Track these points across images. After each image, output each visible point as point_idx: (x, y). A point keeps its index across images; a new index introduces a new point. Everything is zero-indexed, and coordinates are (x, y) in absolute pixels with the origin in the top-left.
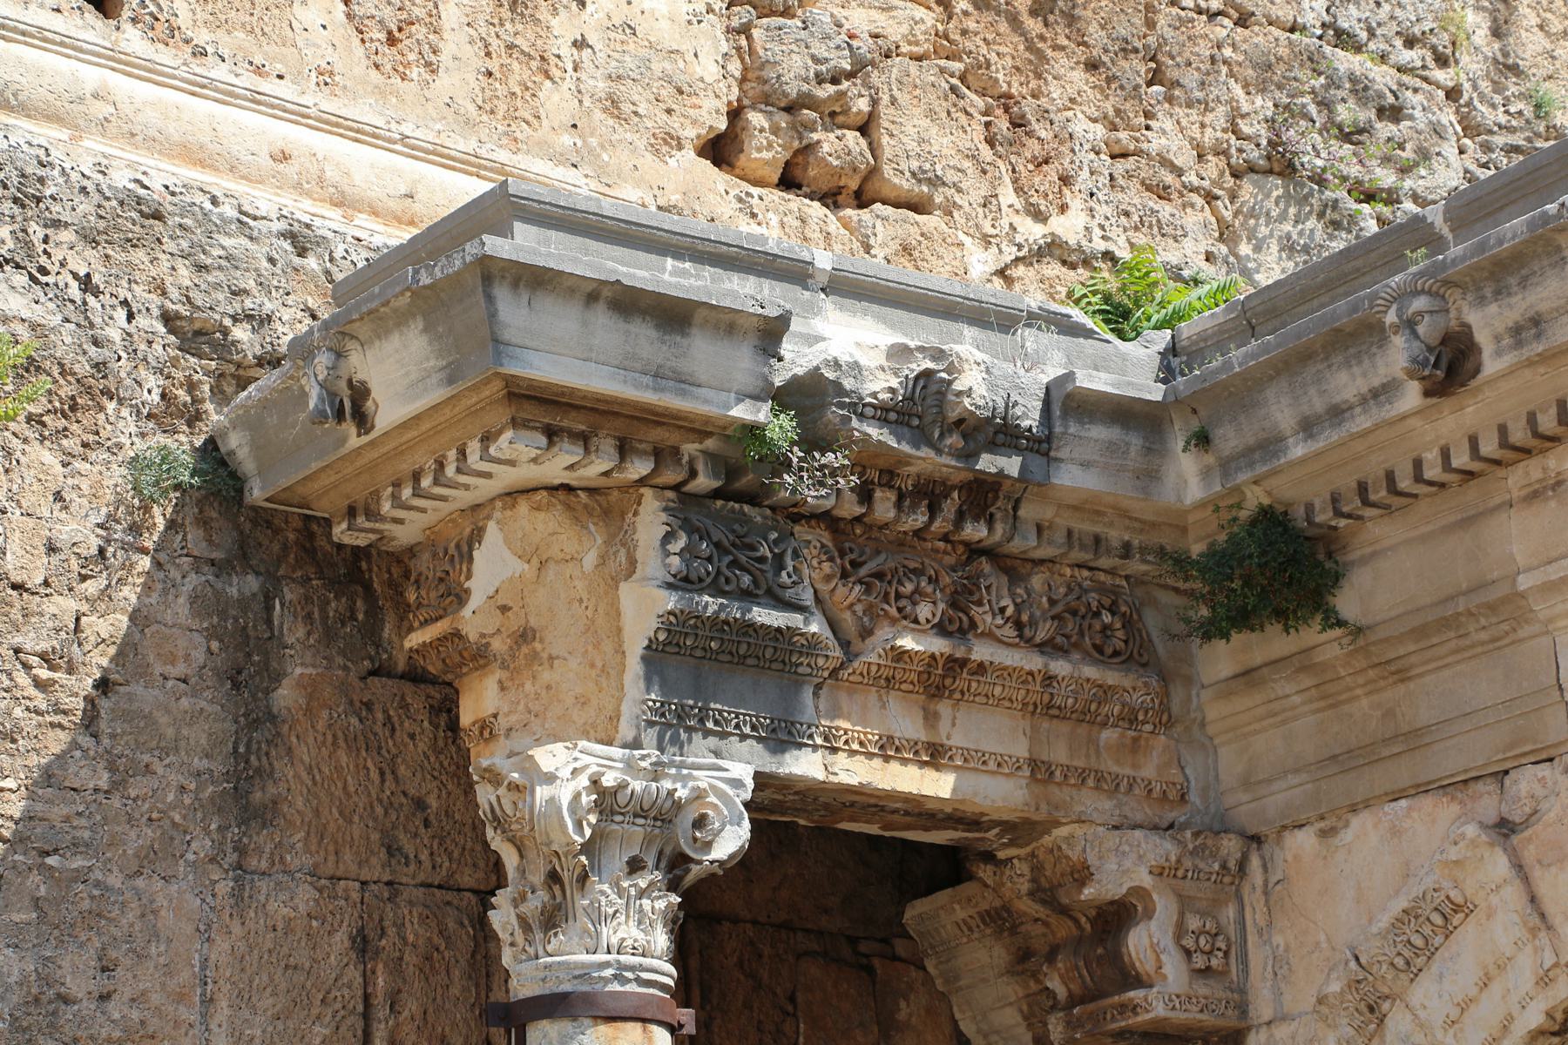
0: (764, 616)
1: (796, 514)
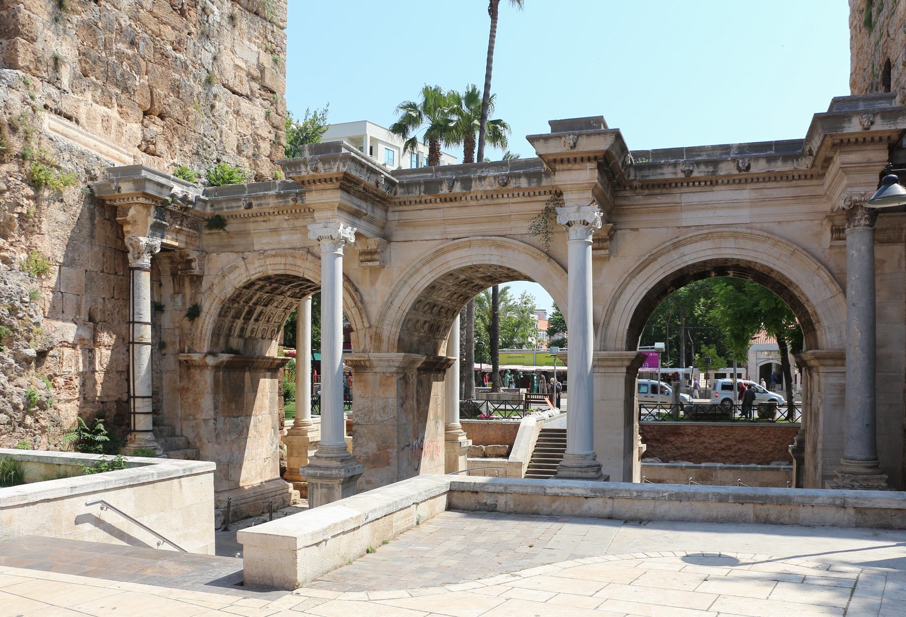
0: (164, 223)
1: (167, 210)
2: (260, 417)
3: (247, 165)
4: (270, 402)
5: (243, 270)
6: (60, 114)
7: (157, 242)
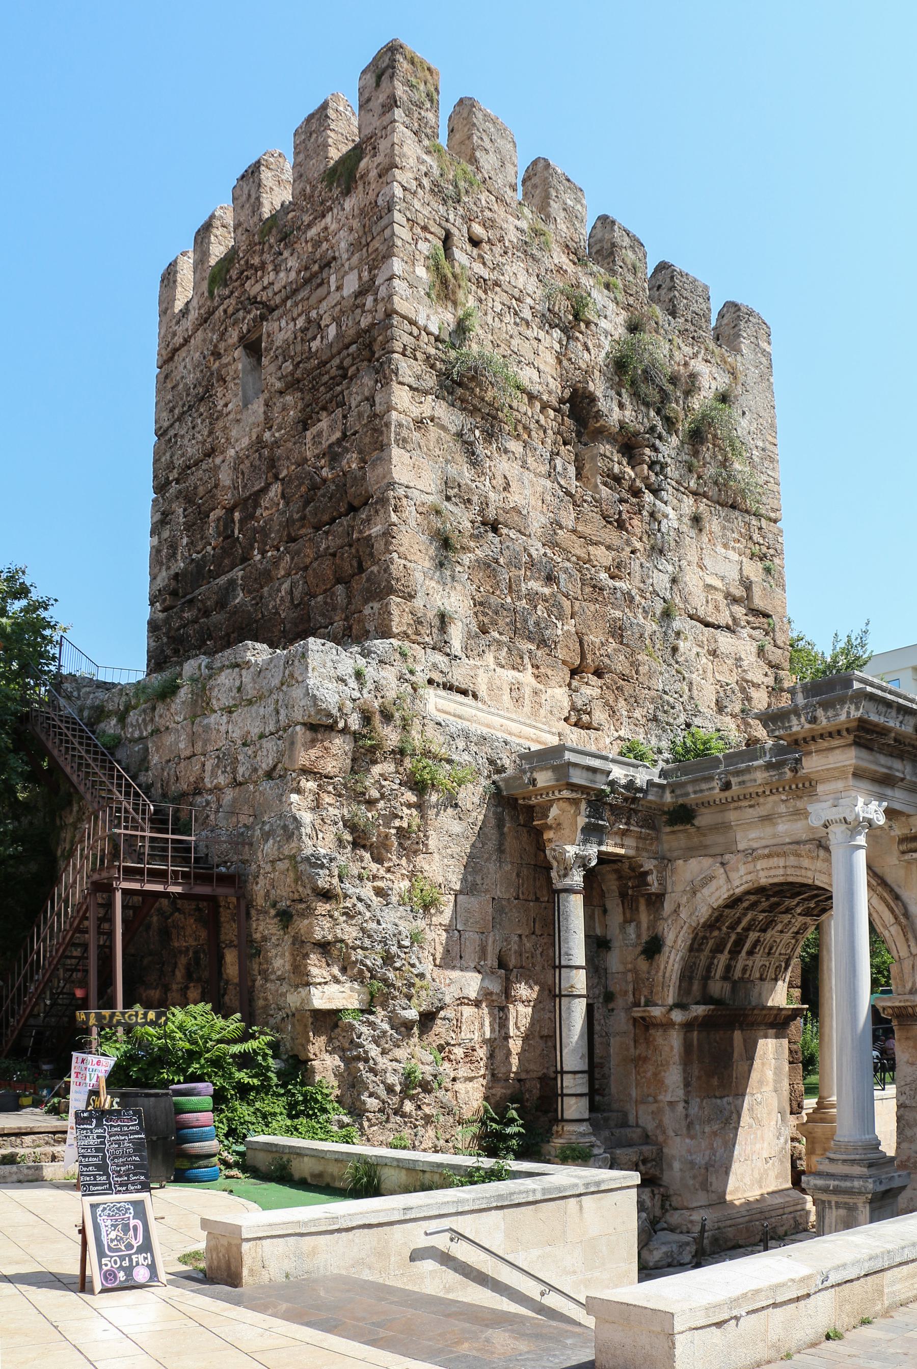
0: (601, 822)
1: (606, 803)
2: (759, 1096)
3: (734, 726)
4: (775, 1074)
5: (722, 880)
7: (592, 851)
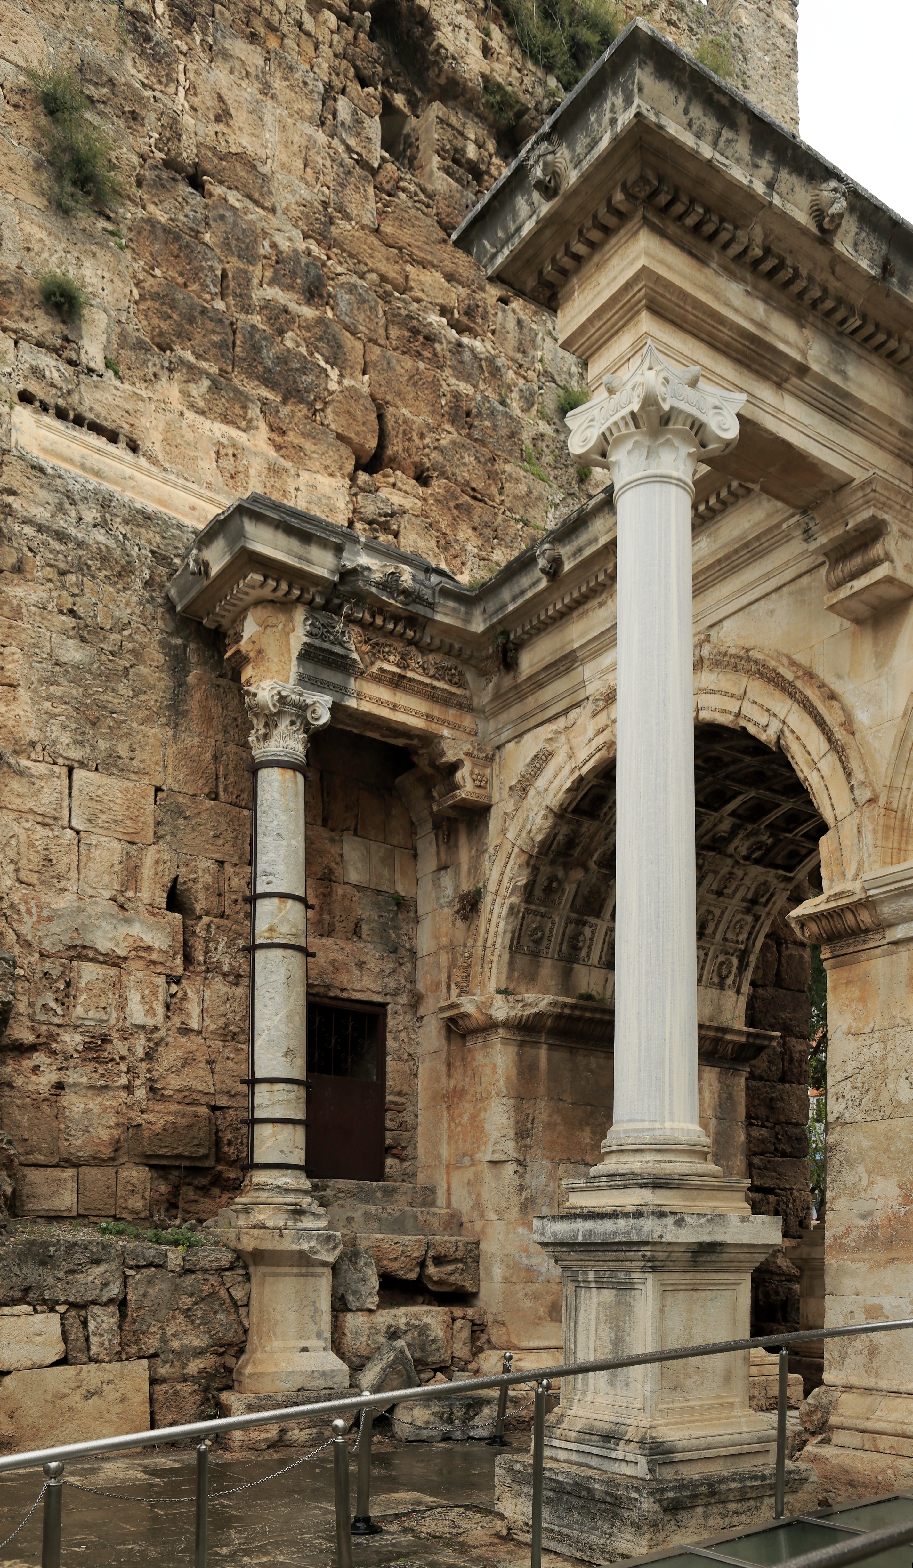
6: (79, 421)
